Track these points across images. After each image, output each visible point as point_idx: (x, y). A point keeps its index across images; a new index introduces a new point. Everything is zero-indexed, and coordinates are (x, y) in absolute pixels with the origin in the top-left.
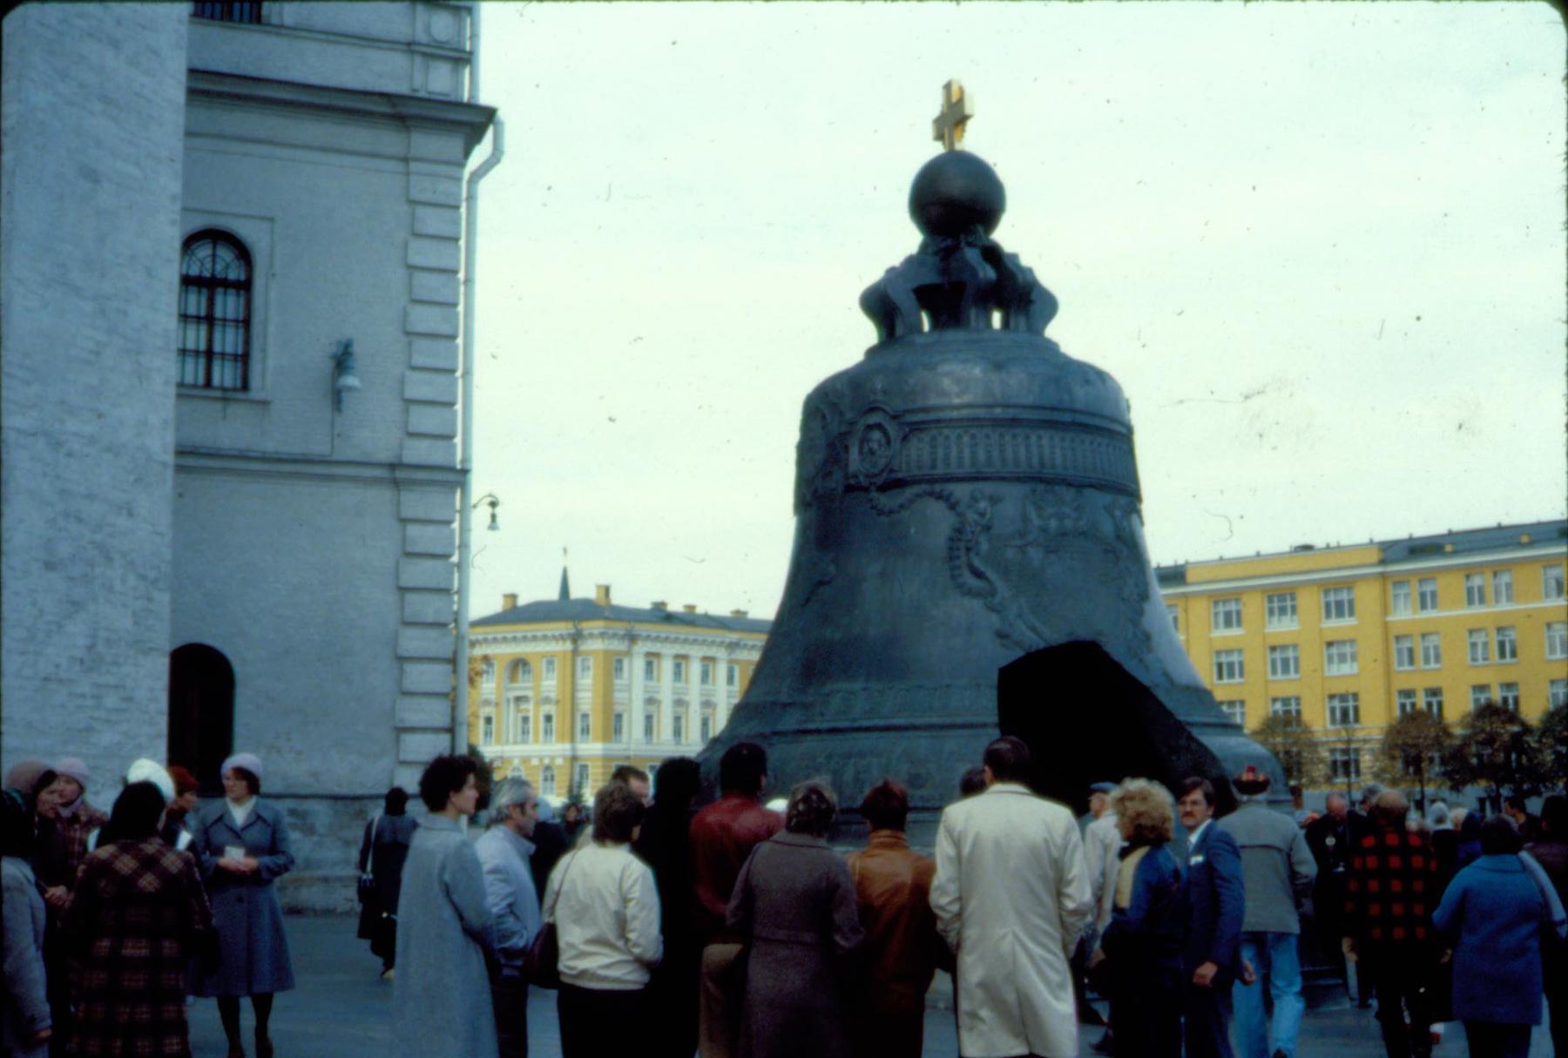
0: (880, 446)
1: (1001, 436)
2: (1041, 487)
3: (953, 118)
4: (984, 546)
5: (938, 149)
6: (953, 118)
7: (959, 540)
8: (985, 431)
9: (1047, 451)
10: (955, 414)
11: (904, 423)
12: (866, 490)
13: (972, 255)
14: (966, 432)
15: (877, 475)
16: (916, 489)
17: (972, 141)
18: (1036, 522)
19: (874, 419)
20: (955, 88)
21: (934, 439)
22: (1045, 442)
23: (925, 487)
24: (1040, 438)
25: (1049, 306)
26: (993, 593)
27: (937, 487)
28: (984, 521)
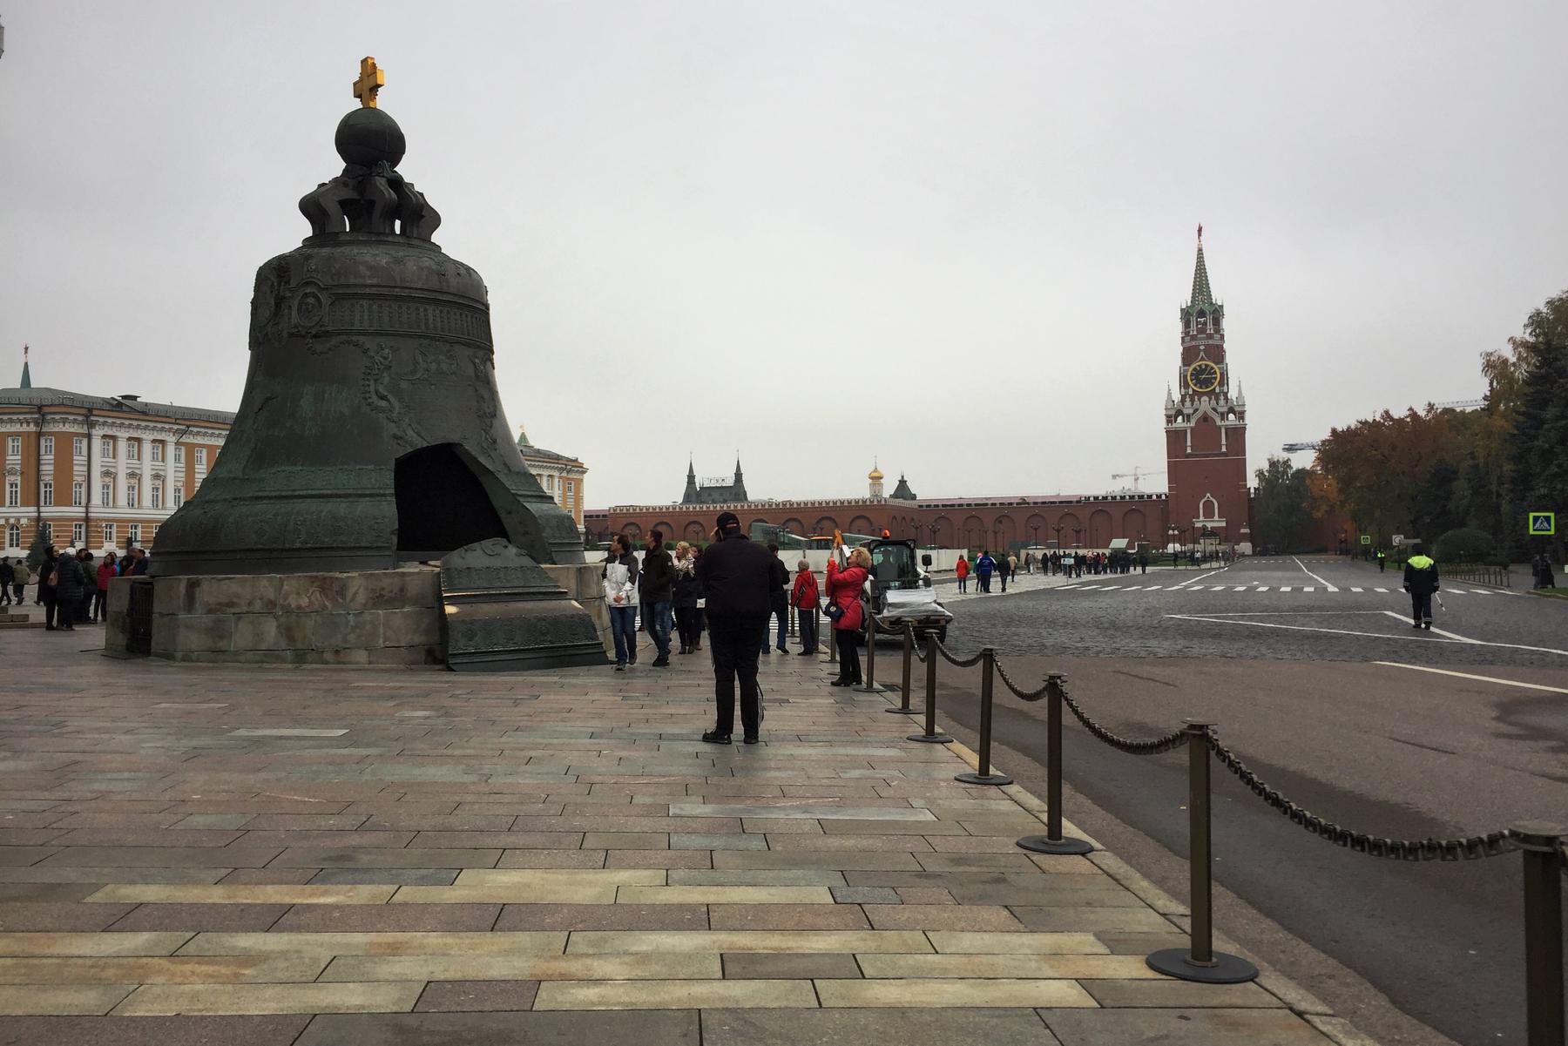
2: (426, 342)
3: (368, 85)
4: (387, 380)
5: (357, 104)
6: (368, 85)
7: (369, 374)
9: (431, 317)
10: (368, 291)
12: (303, 336)
13: (381, 183)
15: (310, 328)
17: (383, 102)
20: (370, 61)
21: (353, 305)
22: (430, 311)
24: (426, 310)
25: (435, 220)
26: (391, 409)
27: (354, 338)
28: (387, 363)
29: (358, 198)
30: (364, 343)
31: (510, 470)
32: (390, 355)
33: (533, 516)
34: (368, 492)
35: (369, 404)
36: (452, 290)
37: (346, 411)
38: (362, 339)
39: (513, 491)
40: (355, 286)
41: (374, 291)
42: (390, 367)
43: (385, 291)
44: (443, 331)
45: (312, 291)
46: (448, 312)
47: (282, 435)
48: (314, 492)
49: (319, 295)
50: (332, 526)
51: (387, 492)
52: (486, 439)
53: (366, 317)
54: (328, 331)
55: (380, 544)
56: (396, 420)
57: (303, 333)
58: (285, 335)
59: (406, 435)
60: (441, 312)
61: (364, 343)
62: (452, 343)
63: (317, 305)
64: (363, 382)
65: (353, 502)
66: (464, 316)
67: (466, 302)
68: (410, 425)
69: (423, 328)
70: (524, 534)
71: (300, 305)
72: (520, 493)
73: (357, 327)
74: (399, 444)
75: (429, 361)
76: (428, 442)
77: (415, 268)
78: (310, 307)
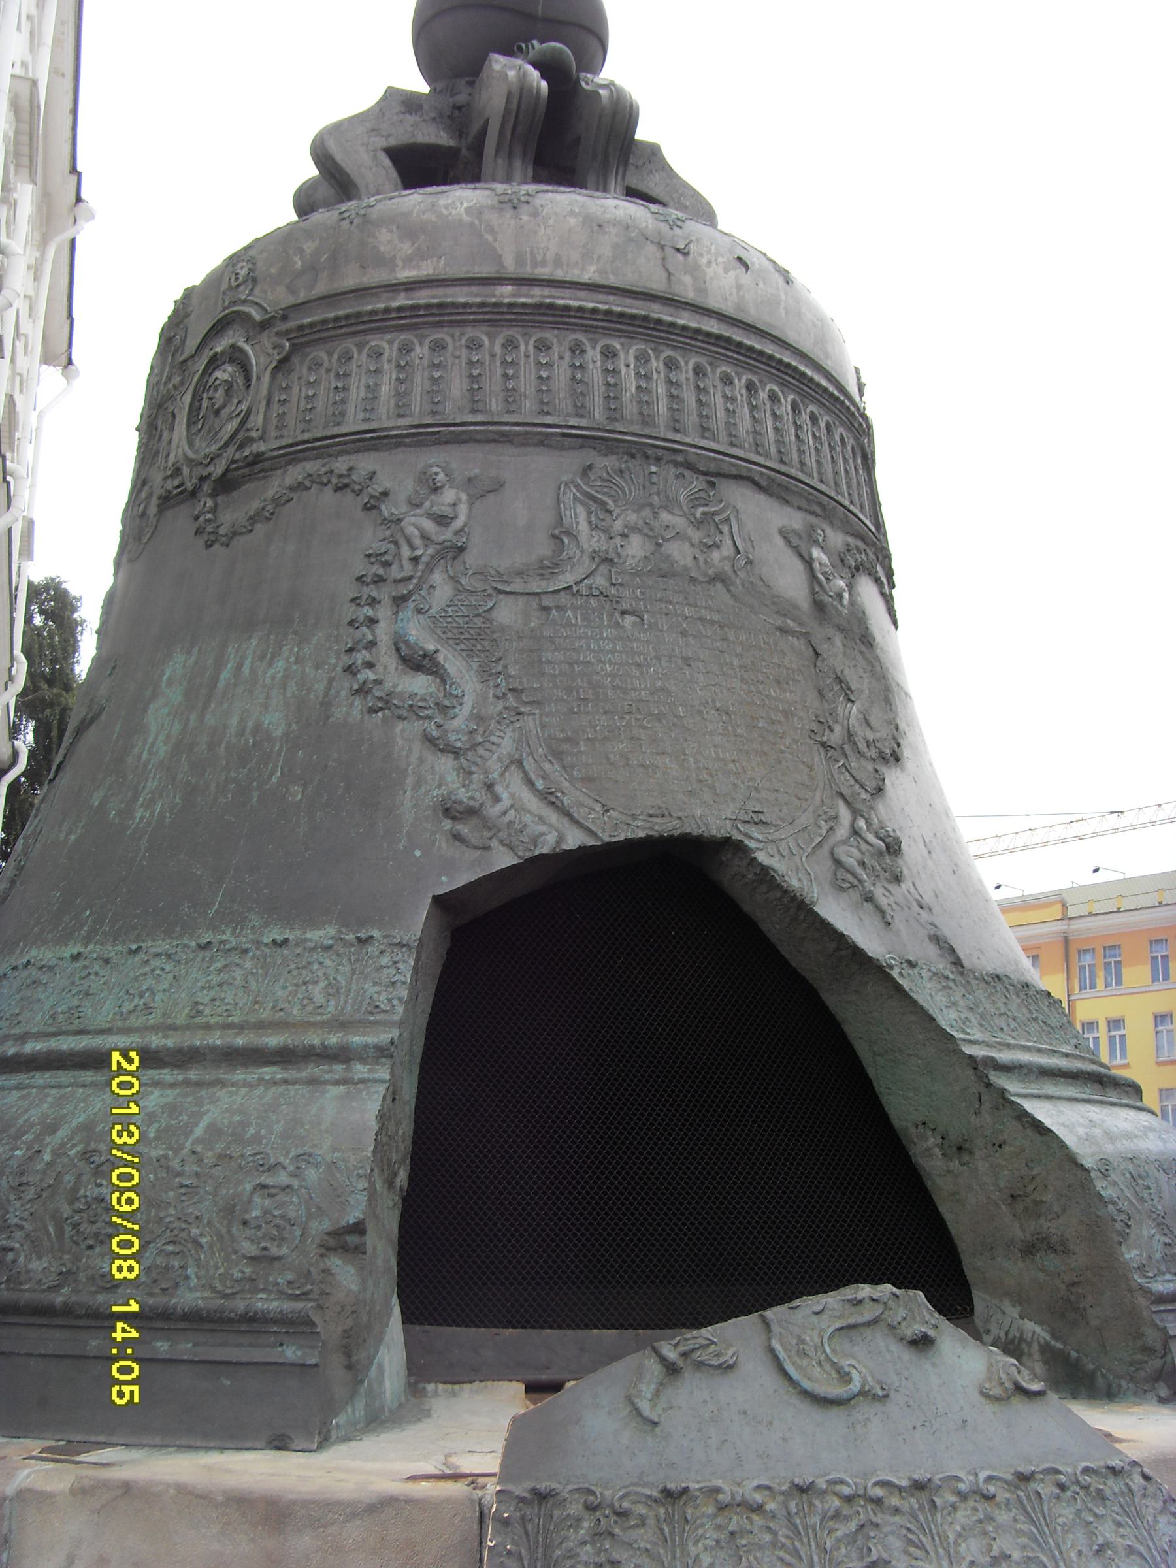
0: (228, 392)
1: (510, 344)
2: (606, 463)
4: (441, 591)
7: (379, 580)
8: (470, 332)
9: (630, 384)
10: (401, 300)
11: (277, 334)
12: (193, 494)
14: (421, 338)
16: (295, 473)
18: (590, 541)
19: (220, 346)
21: (347, 357)
23: (311, 466)
27: (341, 465)
28: (447, 535)
29: (452, 143)
30: (372, 476)
31: (957, 963)
32: (463, 509)
33: (1070, 1159)
34: (273, 1041)
35: (363, 691)
36: (713, 303)
37: (275, 721)
38: (365, 463)
39: (978, 1052)
40: (360, 292)
41: (423, 297)
42: (461, 549)
43: (461, 295)
44: (677, 431)
45: (231, 341)
46: (698, 371)
47: (73, 837)
48: (66, 1044)
49: (247, 348)
50: (73, 1197)
51: (357, 1040)
52: (855, 832)
53: (385, 390)
54: (258, 458)
55: (266, 1303)
56: (458, 740)
57: (189, 486)
58: (153, 510)
59: (497, 799)
60: (671, 365)
61: (372, 476)
62: (714, 476)
63: (241, 381)
64: (350, 612)
65: (199, 1084)
66: (763, 395)
67: (769, 349)
68: (520, 763)
69: (598, 414)
70: (1029, 1250)
71: (196, 398)
72: (1004, 1056)
73: (353, 423)
74: (457, 837)
75: (618, 525)
76: (593, 834)
77: (572, 221)
78: (220, 394)
